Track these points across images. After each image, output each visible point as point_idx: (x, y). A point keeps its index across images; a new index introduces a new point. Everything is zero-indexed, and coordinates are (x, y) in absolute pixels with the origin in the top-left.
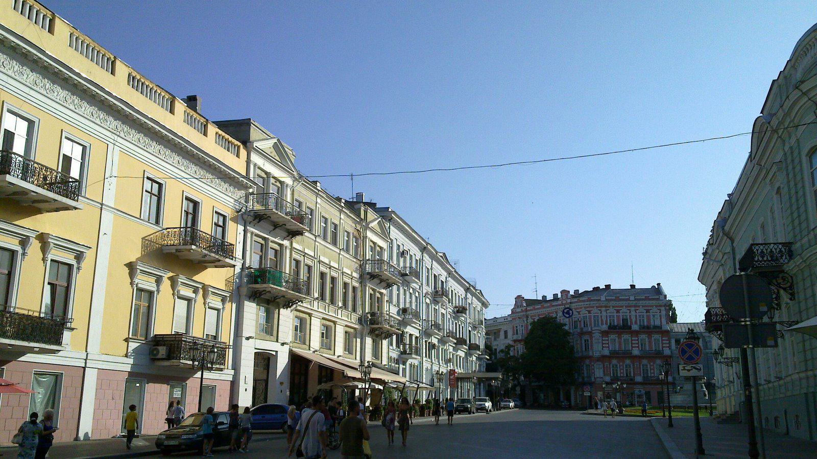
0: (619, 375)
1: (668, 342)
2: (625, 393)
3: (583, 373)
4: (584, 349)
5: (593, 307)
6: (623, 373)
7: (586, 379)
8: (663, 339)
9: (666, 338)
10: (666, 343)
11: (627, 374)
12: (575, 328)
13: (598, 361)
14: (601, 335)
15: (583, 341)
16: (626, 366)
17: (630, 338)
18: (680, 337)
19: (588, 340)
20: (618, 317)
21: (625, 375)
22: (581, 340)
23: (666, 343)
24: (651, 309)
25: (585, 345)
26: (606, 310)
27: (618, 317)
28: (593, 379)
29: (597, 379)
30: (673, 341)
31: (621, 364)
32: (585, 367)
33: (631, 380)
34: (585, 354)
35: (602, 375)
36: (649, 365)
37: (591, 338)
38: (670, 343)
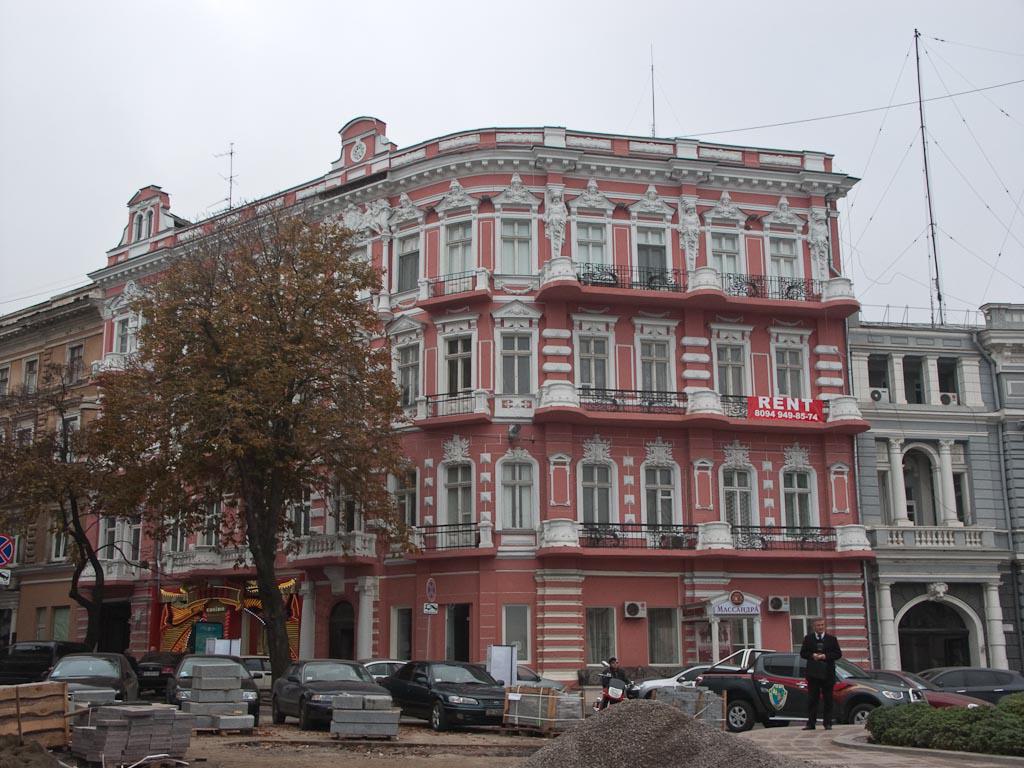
0: (615, 517)
1: (838, 366)
2: (642, 613)
3: (432, 510)
4: (442, 386)
5: (505, 179)
6: (636, 509)
7: (443, 541)
8: (821, 349)
9: (833, 349)
10: (830, 373)
11: (652, 513)
12: (401, 289)
13: (512, 443)
14: (535, 315)
15: (442, 349)
16: (650, 471)
17: (673, 340)
18: (888, 343)
19: (467, 342)
20: (621, 235)
21: (644, 520)
22: (431, 343)
23: (830, 373)
24: (768, 214)
25: (452, 365)
26: (568, 201)
27: (621, 235)
28: (486, 542)
29: (505, 539)
30: (860, 368)
31: (629, 461)
32: (442, 476)
33: (677, 543)
34: (447, 409)
35: (532, 516)
36: (754, 475)
37: (487, 323)
38: (845, 373)
